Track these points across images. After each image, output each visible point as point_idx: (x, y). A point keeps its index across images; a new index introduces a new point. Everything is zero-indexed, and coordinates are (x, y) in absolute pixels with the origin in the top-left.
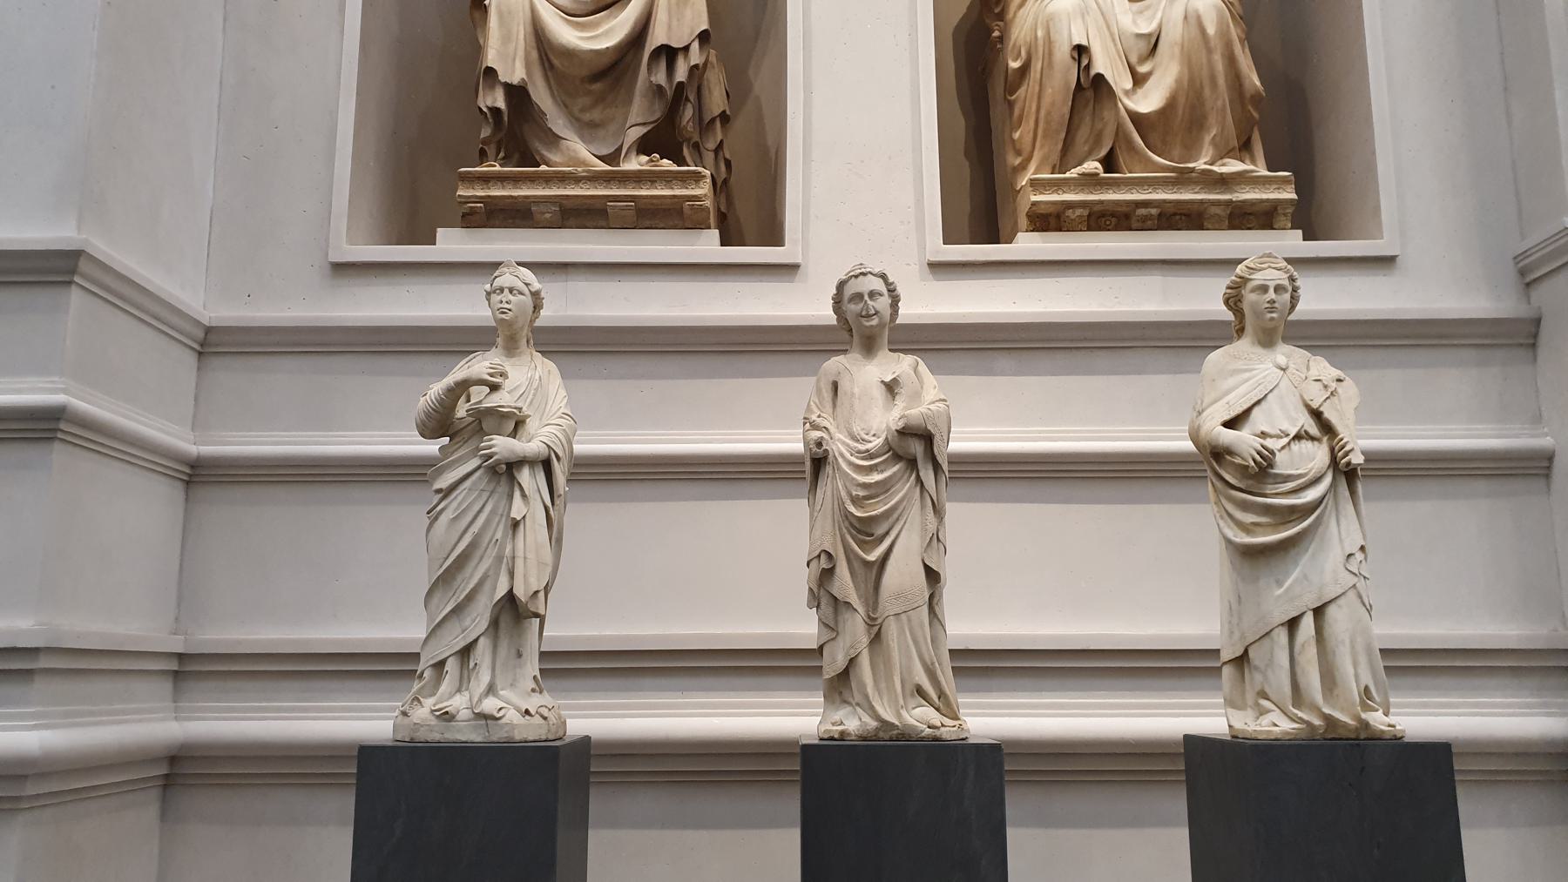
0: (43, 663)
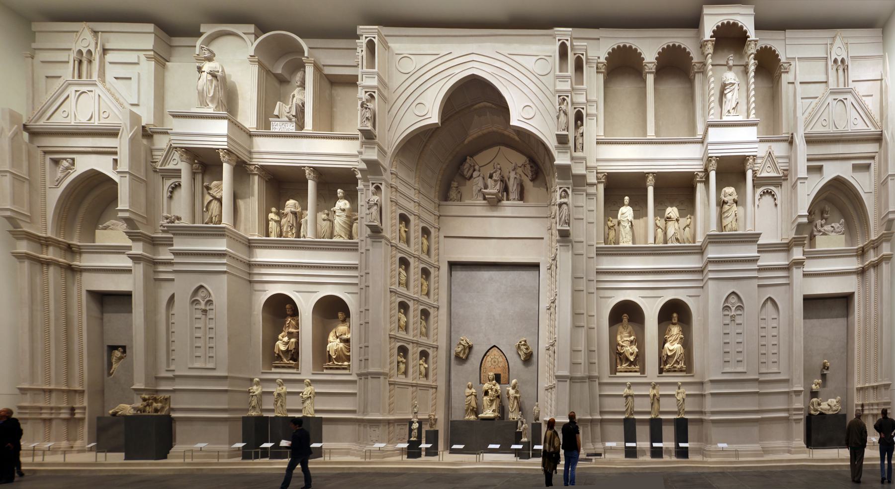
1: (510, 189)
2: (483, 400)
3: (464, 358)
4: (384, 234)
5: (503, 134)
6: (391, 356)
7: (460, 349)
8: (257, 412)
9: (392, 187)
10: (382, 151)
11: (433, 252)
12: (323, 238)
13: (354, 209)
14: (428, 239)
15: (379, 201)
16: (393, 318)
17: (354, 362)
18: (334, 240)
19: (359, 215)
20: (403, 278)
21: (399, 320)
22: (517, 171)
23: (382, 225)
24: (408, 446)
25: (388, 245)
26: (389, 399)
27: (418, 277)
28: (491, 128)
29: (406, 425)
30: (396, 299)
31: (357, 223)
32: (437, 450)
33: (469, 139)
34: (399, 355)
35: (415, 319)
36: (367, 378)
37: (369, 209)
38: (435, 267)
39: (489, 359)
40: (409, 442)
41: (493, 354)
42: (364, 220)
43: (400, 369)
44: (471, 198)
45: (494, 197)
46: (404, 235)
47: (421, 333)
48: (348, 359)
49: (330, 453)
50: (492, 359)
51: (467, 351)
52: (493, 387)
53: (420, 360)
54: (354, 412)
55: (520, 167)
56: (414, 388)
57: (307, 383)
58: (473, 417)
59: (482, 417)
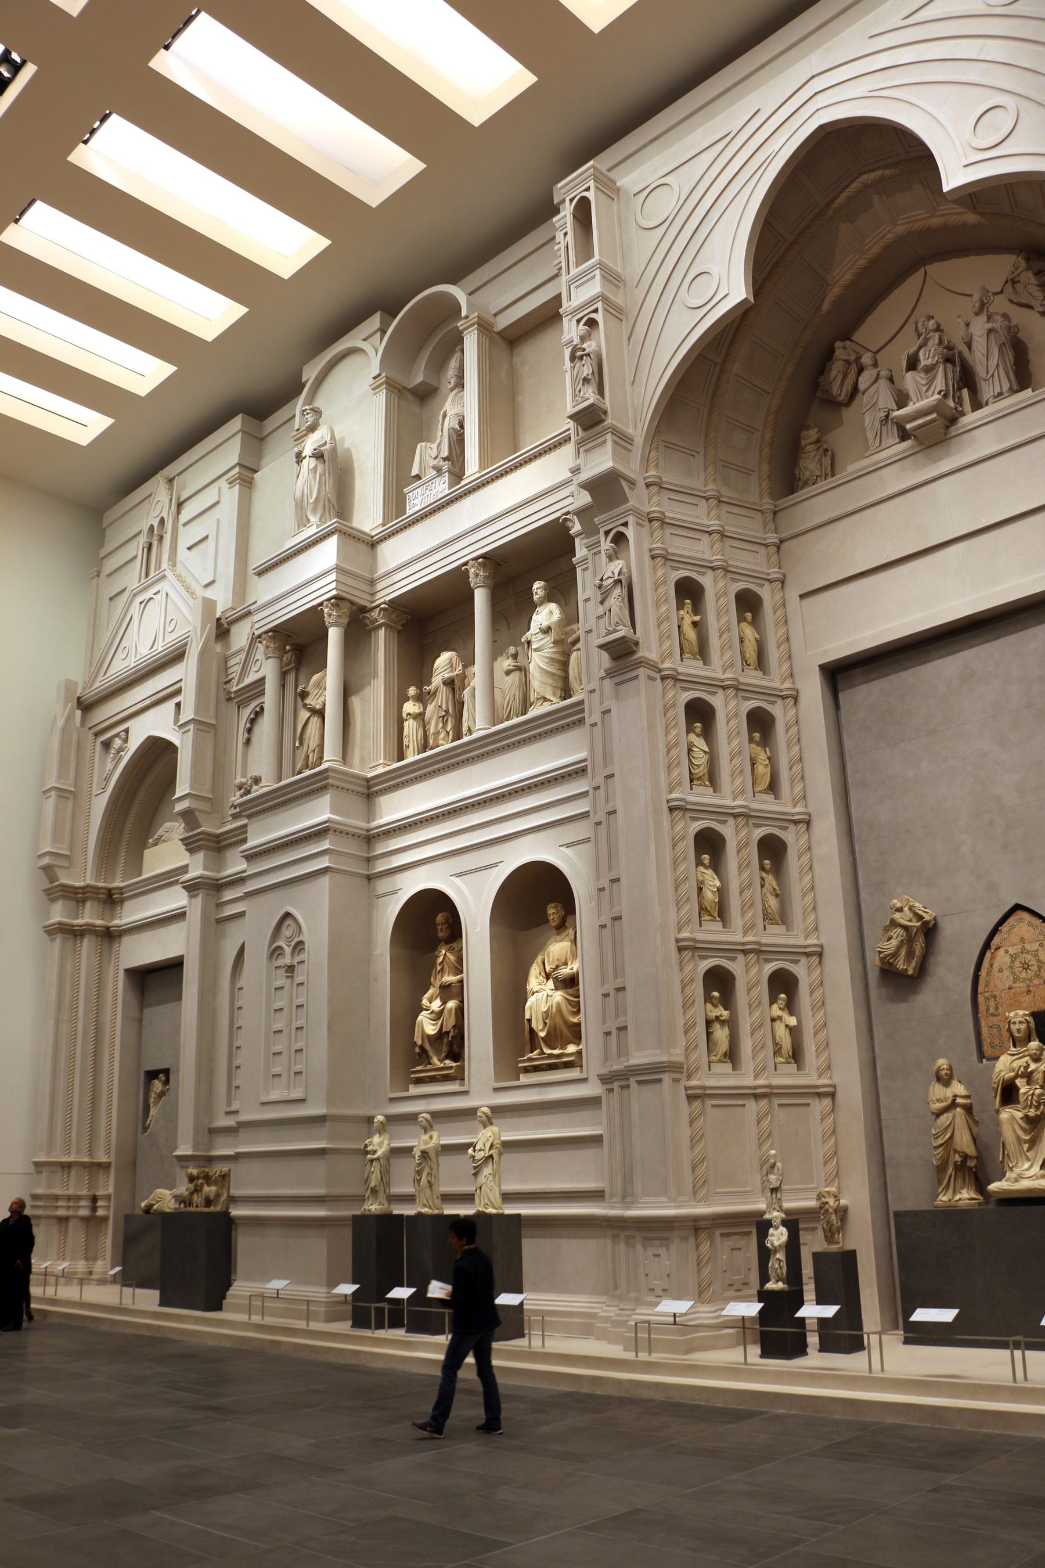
0: (326, 1199)
1: (980, 370)
2: (998, 1123)
3: (910, 972)
4: (642, 653)
5: (929, 229)
6: (686, 1005)
7: (894, 943)
8: (380, 1204)
9: (650, 521)
10: (623, 440)
11: (773, 655)
12: (508, 719)
13: (571, 617)
14: (755, 623)
15: (625, 570)
16: (684, 888)
17: (592, 1043)
18: (532, 713)
19: (581, 628)
20: (701, 760)
21: (700, 889)
22: (992, 309)
23: (635, 633)
24: (761, 1312)
25: (653, 679)
26: (692, 1148)
27: (740, 743)
28: (889, 232)
29: (749, 1233)
30: (686, 827)
31: (579, 649)
32: (861, 1328)
33: (835, 292)
34: (708, 999)
35: (746, 874)
36: (628, 1087)
37: (602, 602)
38: (783, 698)
39: (1002, 959)
40: (763, 1296)
41: (1015, 939)
42: (594, 634)
43: (716, 1044)
44: (865, 449)
45: (934, 416)
46: (691, 634)
47: (766, 916)
48: (575, 1033)
49: (543, 1325)
50: (1014, 958)
51: (919, 946)
52: (1033, 1066)
53: (772, 1003)
54: (596, 1195)
55: (1001, 292)
56: (764, 1103)
57: (484, 1118)
58: (965, 1196)
59: (1004, 1191)
